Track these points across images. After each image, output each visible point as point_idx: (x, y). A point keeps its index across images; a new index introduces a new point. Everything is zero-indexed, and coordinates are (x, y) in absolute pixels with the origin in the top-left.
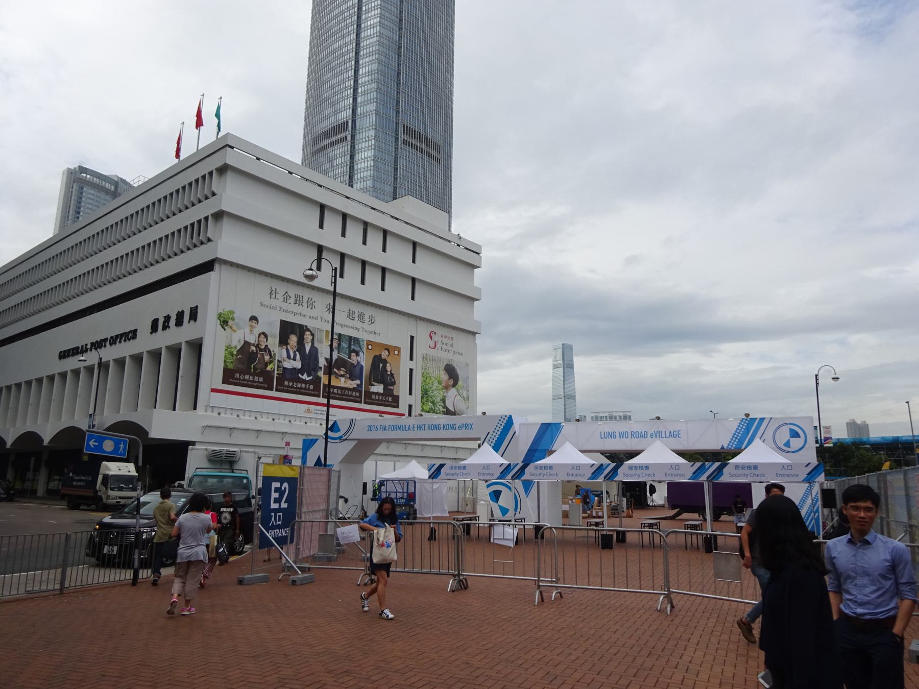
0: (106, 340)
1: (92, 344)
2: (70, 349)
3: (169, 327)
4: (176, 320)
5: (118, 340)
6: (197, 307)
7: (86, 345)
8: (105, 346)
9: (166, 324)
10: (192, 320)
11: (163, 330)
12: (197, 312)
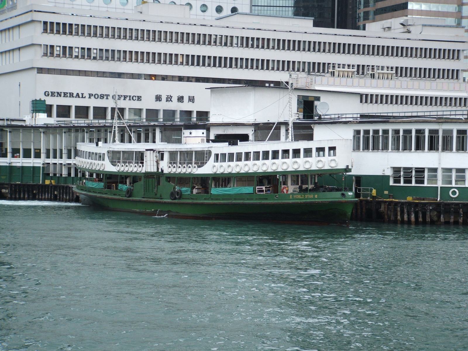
0: (107, 96)
1: (90, 95)
2: (61, 93)
3: (172, 101)
4: (178, 99)
5: (123, 98)
6: (194, 97)
7: (82, 94)
8: (107, 98)
9: (169, 99)
10: (190, 101)
11: (167, 101)
12: (194, 99)
